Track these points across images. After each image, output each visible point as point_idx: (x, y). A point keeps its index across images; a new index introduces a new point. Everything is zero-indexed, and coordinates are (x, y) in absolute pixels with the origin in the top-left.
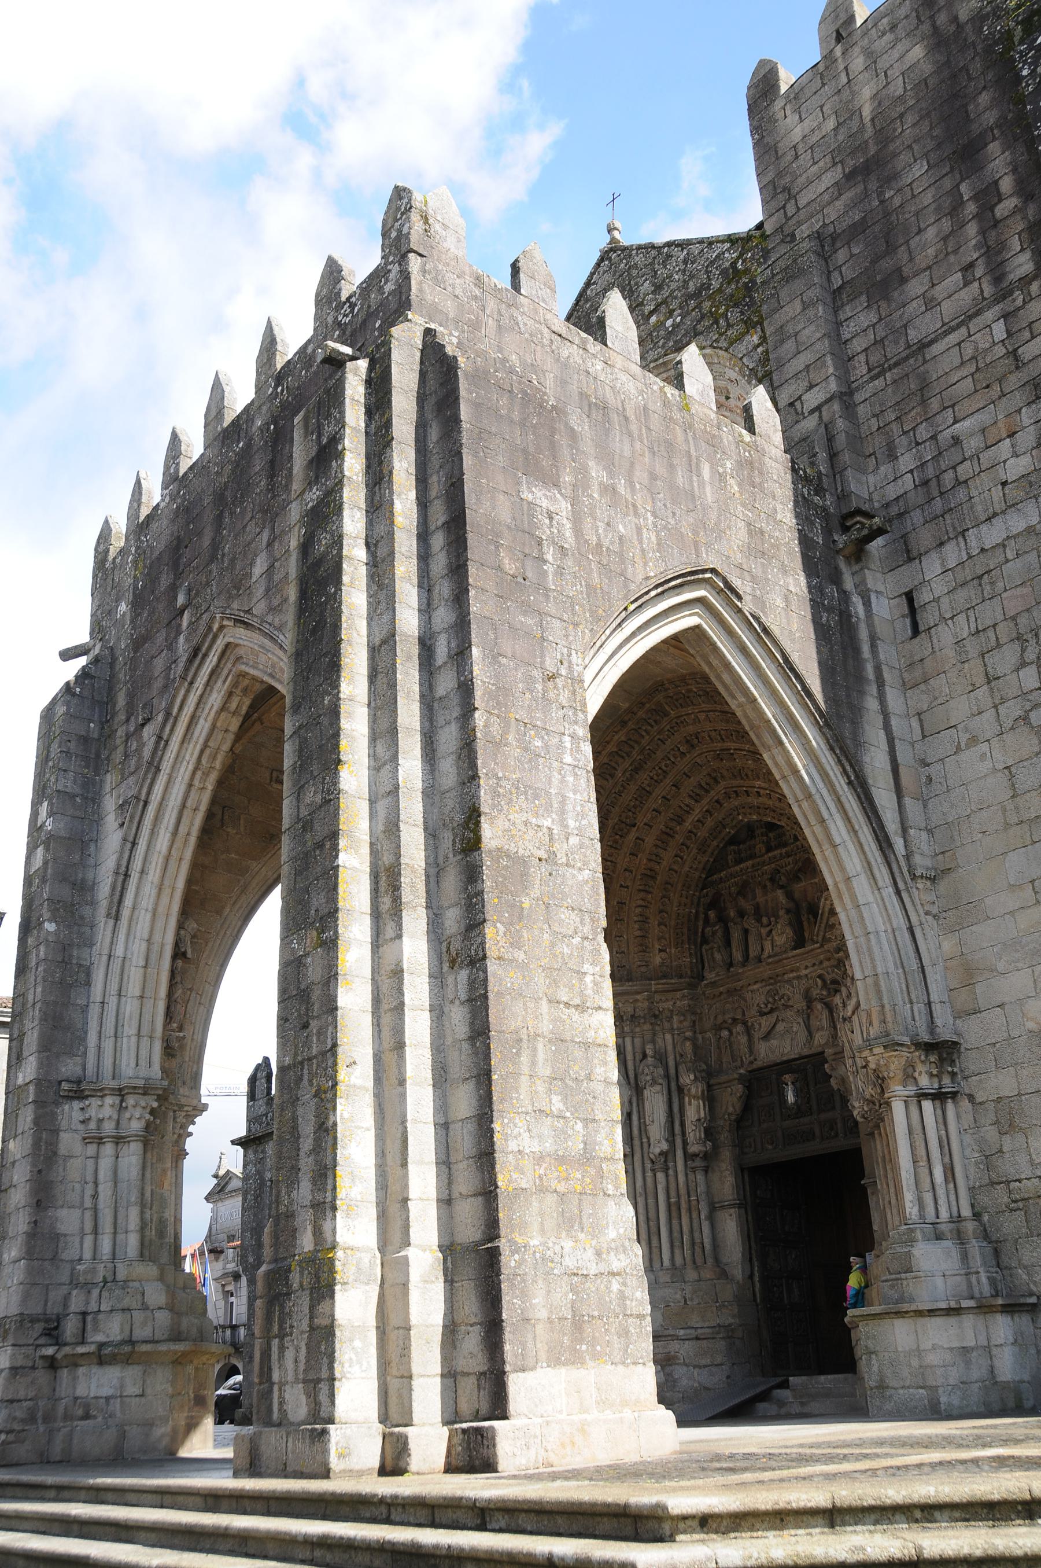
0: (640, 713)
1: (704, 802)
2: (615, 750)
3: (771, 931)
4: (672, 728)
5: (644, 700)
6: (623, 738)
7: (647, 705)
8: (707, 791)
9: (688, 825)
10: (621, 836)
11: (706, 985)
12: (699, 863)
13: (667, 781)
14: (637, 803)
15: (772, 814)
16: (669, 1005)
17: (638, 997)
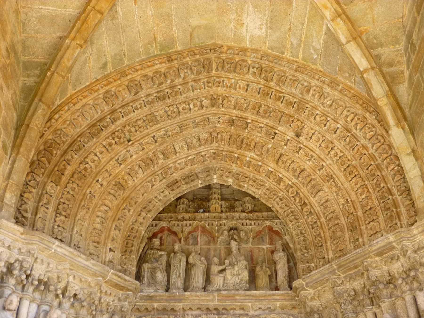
0: (187, 59)
1: (193, 152)
2: (151, 75)
3: (224, 270)
4: (208, 82)
5: (197, 52)
6: (163, 70)
7: (198, 57)
8: (200, 146)
9: (170, 162)
10: (116, 143)
11: (142, 298)
12: (165, 196)
13: (175, 121)
14: (144, 124)
15: (251, 182)
16: (110, 299)
17: (90, 279)
